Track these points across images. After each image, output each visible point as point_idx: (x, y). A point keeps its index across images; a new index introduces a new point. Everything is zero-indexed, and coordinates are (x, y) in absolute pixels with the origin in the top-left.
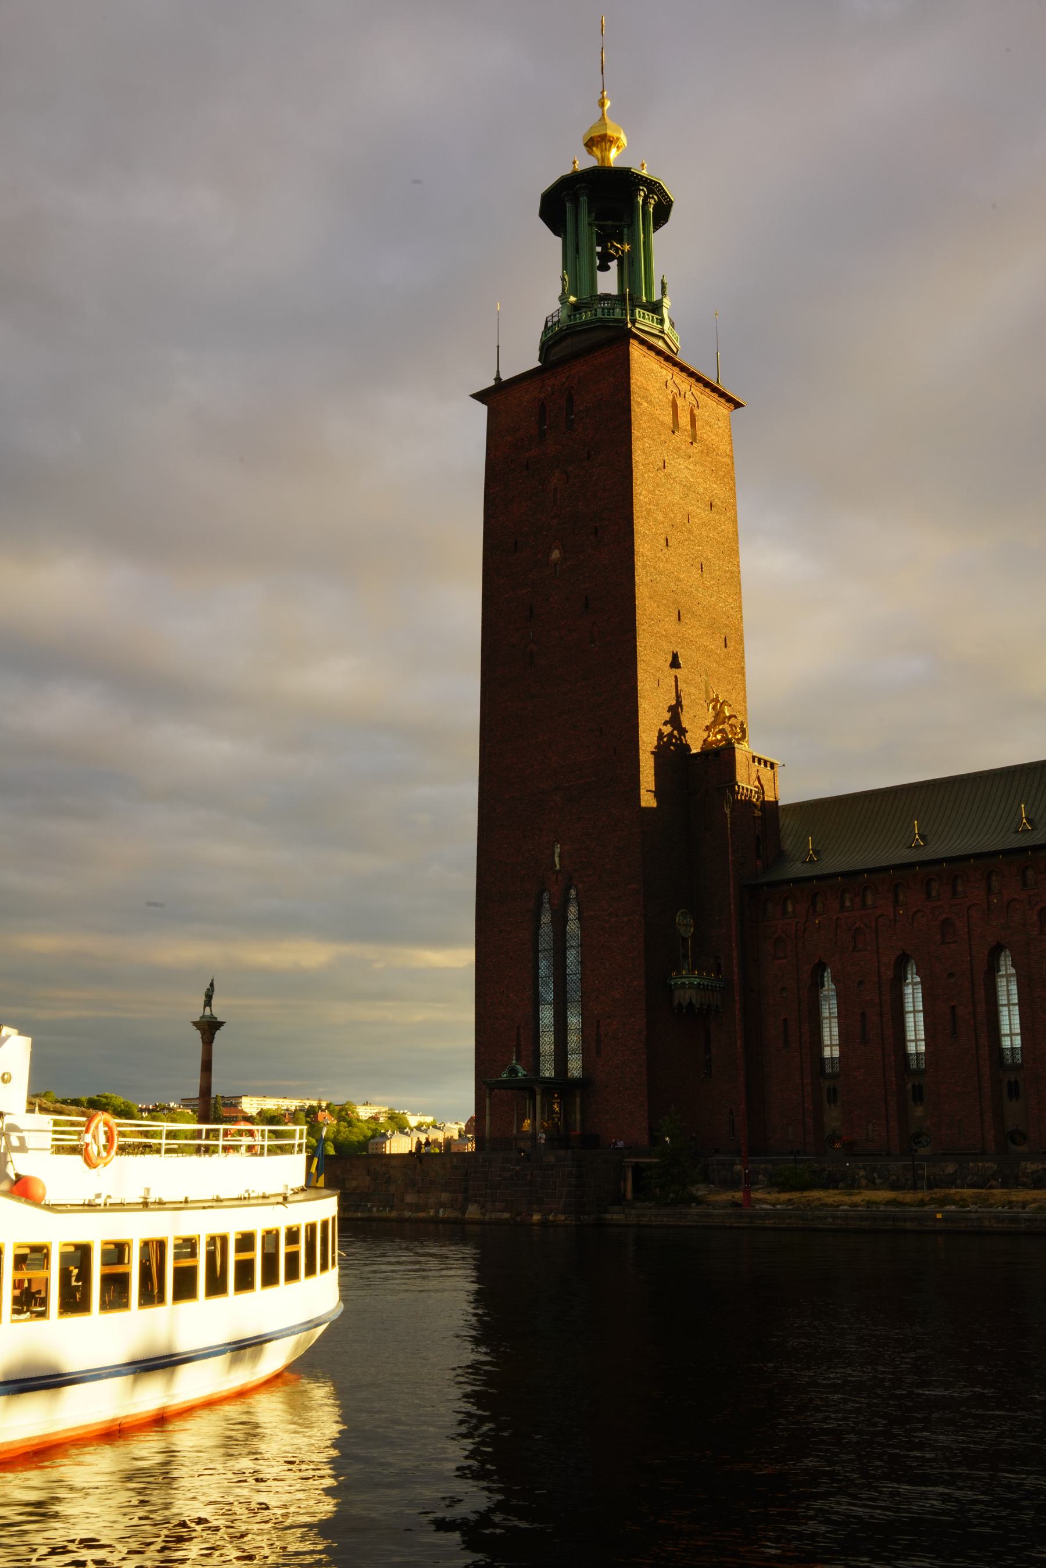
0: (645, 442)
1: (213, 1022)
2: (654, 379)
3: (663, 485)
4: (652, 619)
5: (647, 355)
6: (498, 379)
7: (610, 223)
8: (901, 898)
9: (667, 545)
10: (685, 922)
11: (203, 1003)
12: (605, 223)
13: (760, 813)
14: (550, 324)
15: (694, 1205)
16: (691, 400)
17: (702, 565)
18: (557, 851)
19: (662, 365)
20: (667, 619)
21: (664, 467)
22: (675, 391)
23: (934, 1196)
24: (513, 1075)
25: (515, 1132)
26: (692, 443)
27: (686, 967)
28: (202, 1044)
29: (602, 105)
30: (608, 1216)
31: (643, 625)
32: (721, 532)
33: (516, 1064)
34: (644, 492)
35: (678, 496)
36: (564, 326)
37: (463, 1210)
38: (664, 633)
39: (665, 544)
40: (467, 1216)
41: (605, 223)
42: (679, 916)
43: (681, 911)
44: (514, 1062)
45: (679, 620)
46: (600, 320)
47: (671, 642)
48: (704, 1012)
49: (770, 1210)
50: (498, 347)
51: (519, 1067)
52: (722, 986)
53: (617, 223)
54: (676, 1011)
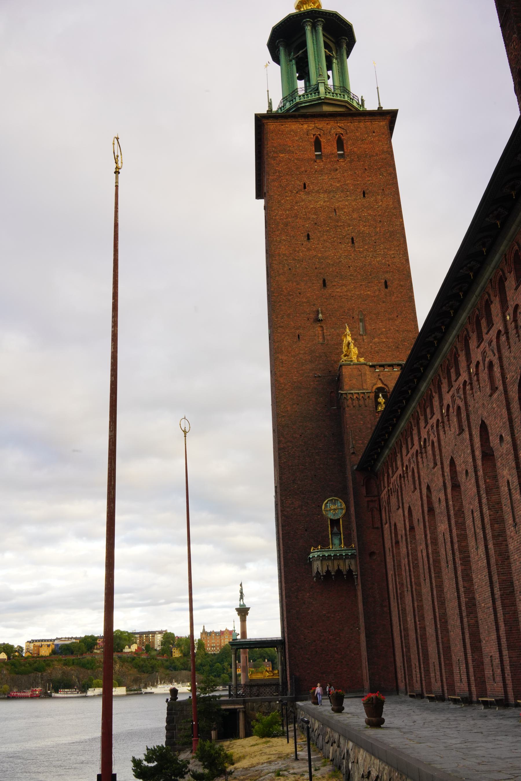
0: (282, 179)
3: (303, 200)
4: (290, 295)
5: (284, 123)
7: (301, 52)
9: (309, 238)
10: (333, 507)
17: (352, 239)
19: (302, 123)
21: (305, 188)
26: (338, 161)
27: (336, 542)
31: (279, 302)
32: (378, 207)
38: (305, 300)
39: (306, 239)
42: (327, 503)
47: (314, 305)
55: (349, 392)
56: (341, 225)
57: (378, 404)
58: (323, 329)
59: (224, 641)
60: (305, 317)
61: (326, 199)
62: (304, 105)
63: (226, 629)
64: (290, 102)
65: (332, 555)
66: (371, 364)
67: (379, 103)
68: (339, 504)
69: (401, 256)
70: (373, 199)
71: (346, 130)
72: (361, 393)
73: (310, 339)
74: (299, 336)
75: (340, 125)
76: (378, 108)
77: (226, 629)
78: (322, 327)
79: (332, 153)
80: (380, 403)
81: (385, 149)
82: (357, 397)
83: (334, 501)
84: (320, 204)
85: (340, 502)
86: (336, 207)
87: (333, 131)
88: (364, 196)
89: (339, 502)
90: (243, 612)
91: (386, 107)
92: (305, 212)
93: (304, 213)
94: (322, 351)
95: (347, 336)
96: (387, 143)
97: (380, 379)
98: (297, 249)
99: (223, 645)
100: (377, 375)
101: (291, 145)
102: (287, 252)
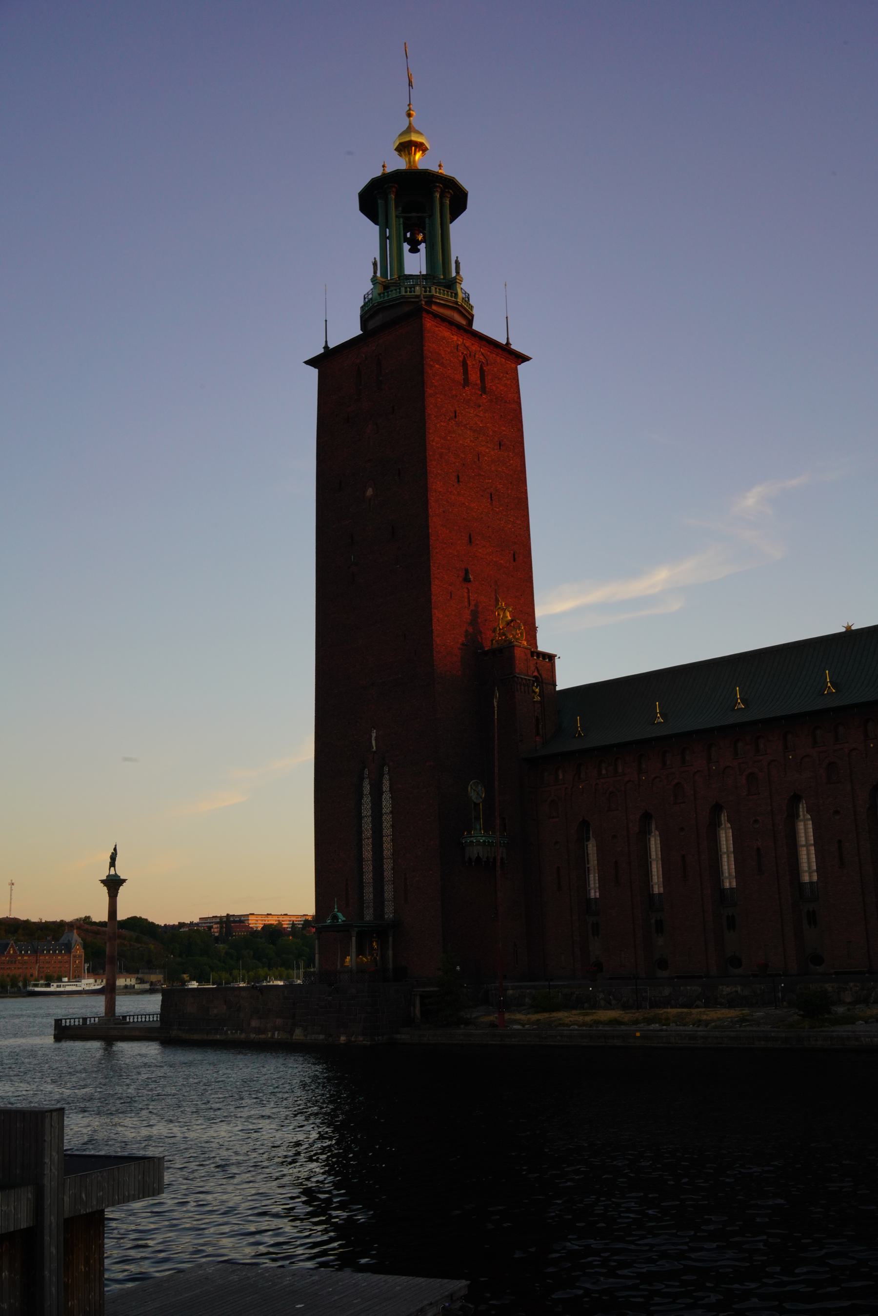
1: (116, 880)
6: (326, 347)
7: (414, 214)
8: (644, 766)
9: (459, 481)
12: (410, 215)
13: (539, 698)
14: (367, 300)
15: (462, 1026)
16: (481, 359)
17: (491, 495)
18: (374, 735)
20: (459, 542)
21: (455, 417)
22: (465, 352)
23: (646, 1015)
24: (335, 921)
25: (339, 967)
26: (481, 395)
28: (108, 898)
29: (409, 115)
30: (398, 1036)
32: (510, 466)
33: (338, 912)
34: (436, 439)
35: (469, 439)
36: (375, 303)
37: (291, 1032)
38: (456, 554)
39: (456, 480)
40: (294, 1037)
41: (410, 215)
43: (473, 781)
44: (336, 910)
45: (470, 542)
46: (403, 297)
47: (462, 561)
49: (521, 1030)
50: (326, 321)
51: (340, 915)
52: (506, 842)
53: (419, 215)
54: (467, 864)
61: (472, 439)
62: (438, 301)
67: (508, 338)
80: (535, 693)
81: (515, 398)
84: (467, 443)
85: (481, 786)
87: (477, 356)
88: (500, 448)
90: (113, 884)
95: (506, 611)
98: (450, 490)
100: (535, 662)
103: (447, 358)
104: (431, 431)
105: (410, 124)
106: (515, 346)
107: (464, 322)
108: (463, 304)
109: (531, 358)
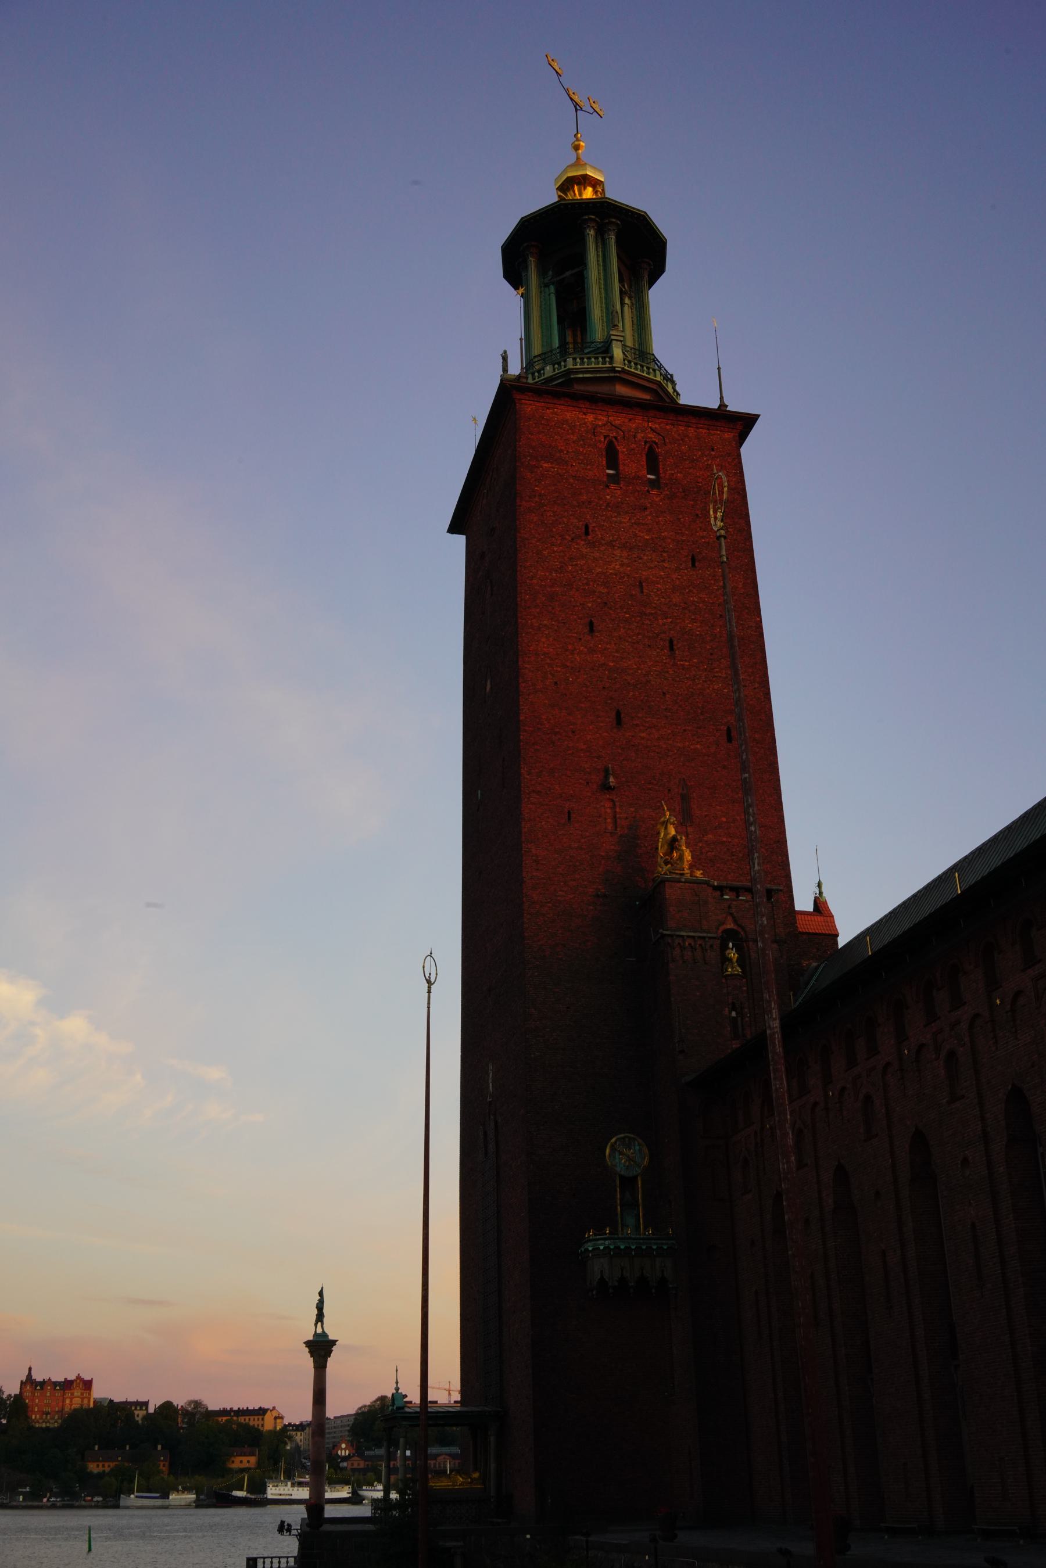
0: (545, 511)
2: (568, 431)
5: (552, 406)
7: (568, 273)
11: (315, 1317)
12: (565, 276)
16: (651, 438)
17: (671, 642)
21: (587, 533)
26: (648, 491)
29: (577, 148)
32: (717, 590)
41: (565, 276)
42: (615, 1142)
48: (653, 1291)
55: (678, 933)
56: (651, 614)
57: (725, 960)
58: (614, 805)
59: (71, 1401)
60: (581, 779)
61: (625, 561)
62: (581, 376)
63: (78, 1377)
64: (554, 365)
65: (633, 1247)
66: (716, 884)
67: (722, 398)
68: (637, 1148)
69: (757, 685)
70: (708, 573)
71: (663, 437)
72: (700, 937)
73: (590, 821)
74: (569, 813)
75: (653, 427)
76: (720, 406)
77: (78, 1377)
78: (612, 801)
79: (639, 477)
80: (730, 960)
82: (690, 944)
83: (627, 1139)
85: (639, 1145)
86: (643, 577)
87: (640, 436)
88: (693, 565)
89: (637, 1144)
91: (735, 405)
92: (586, 578)
93: (585, 582)
94: (612, 847)
95: (669, 825)
96: (735, 474)
97: (731, 914)
98: (570, 647)
99: (67, 1409)
101: (563, 448)
102: (552, 650)
103: (570, 450)
104: (528, 564)
105: (578, 158)
106: (733, 407)
107: (646, 396)
108: (626, 368)
109: (758, 416)
